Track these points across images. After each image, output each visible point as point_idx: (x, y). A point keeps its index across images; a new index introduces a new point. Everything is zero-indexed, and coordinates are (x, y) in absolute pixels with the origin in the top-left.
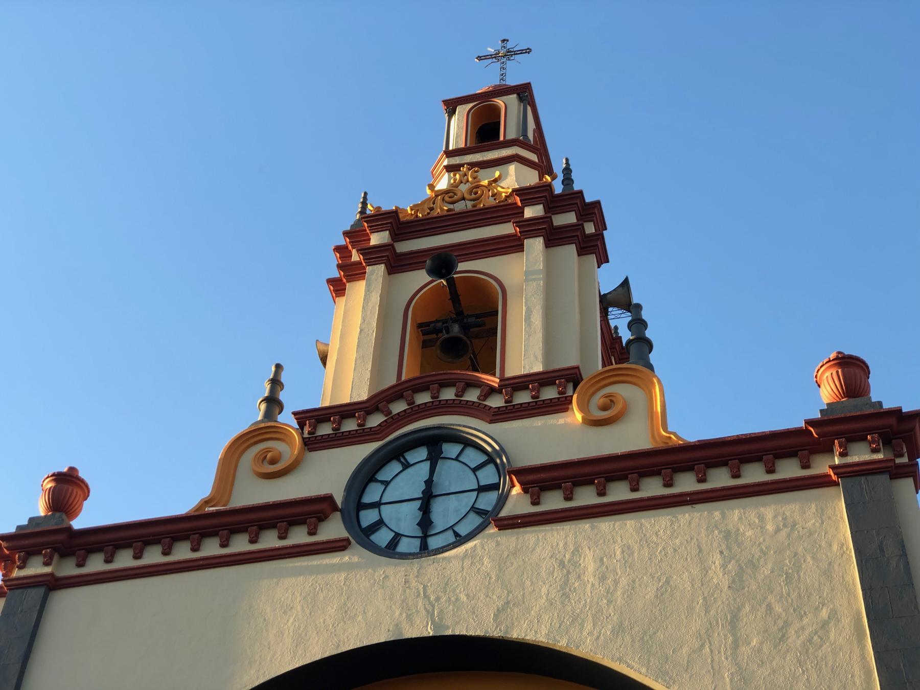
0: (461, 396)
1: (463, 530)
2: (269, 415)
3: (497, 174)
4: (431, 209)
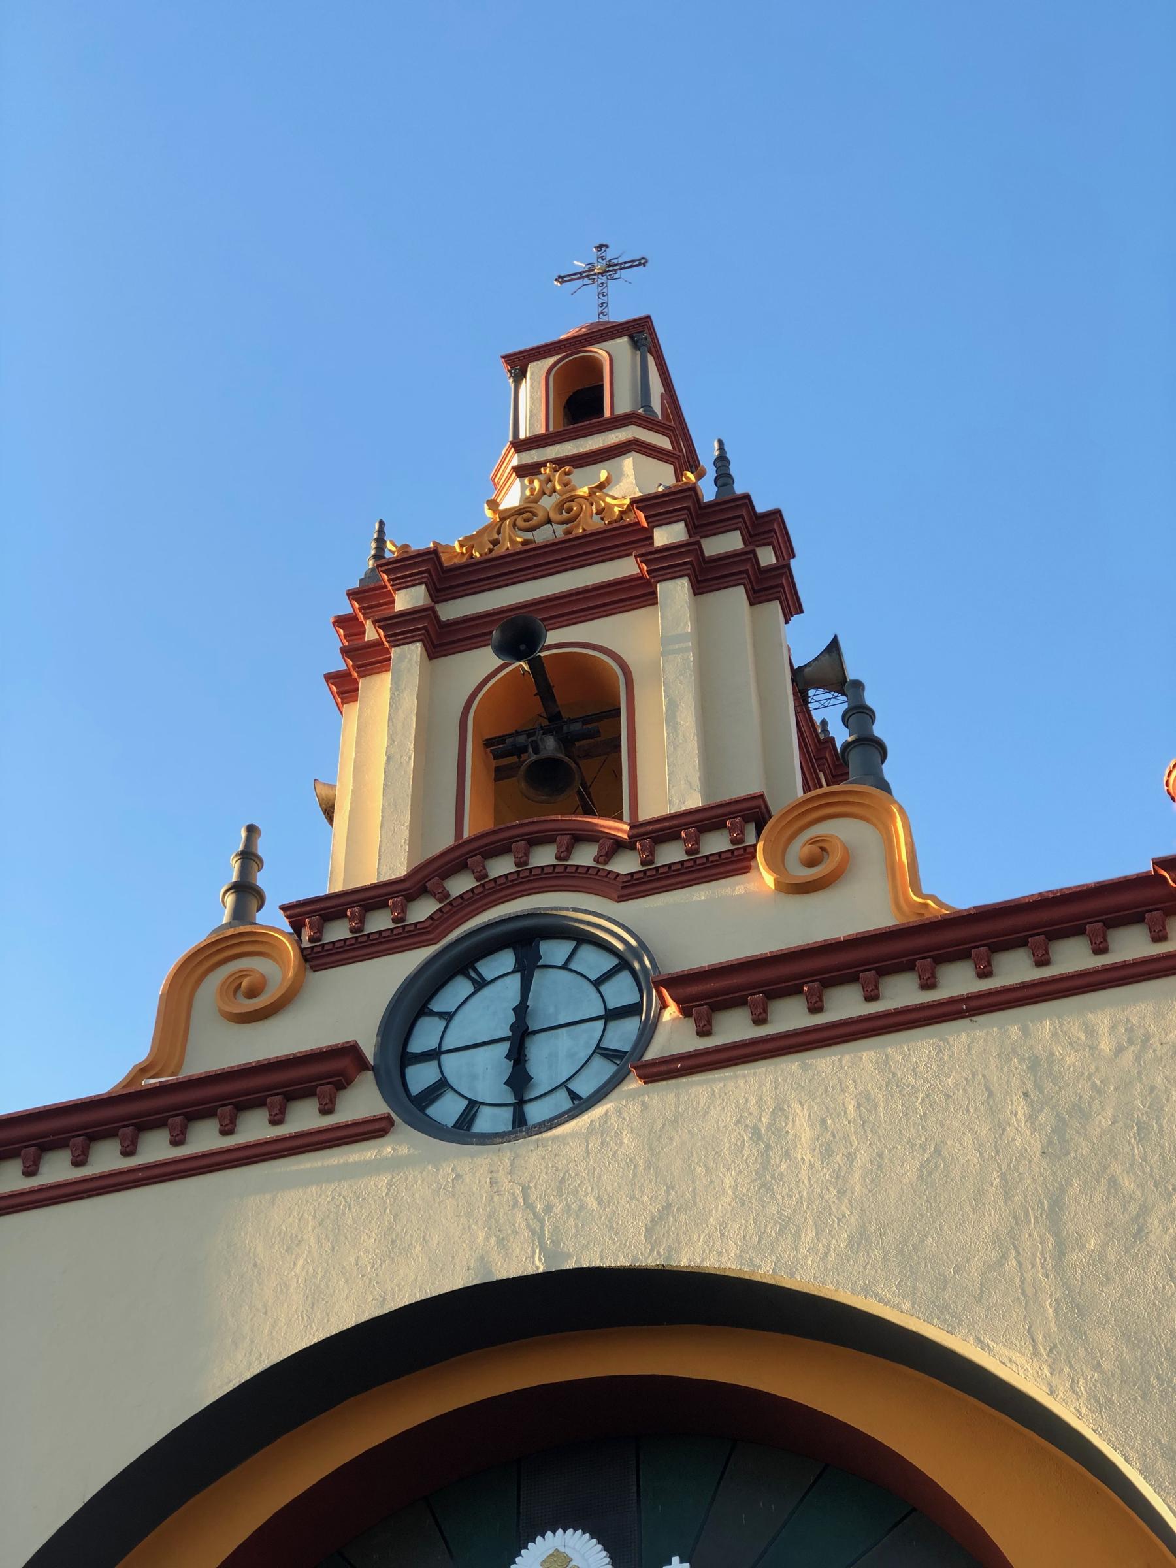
0: (566, 859)
1: (584, 1088)
2: (240, 914)
3: (603, 475)
4: (495, 543)
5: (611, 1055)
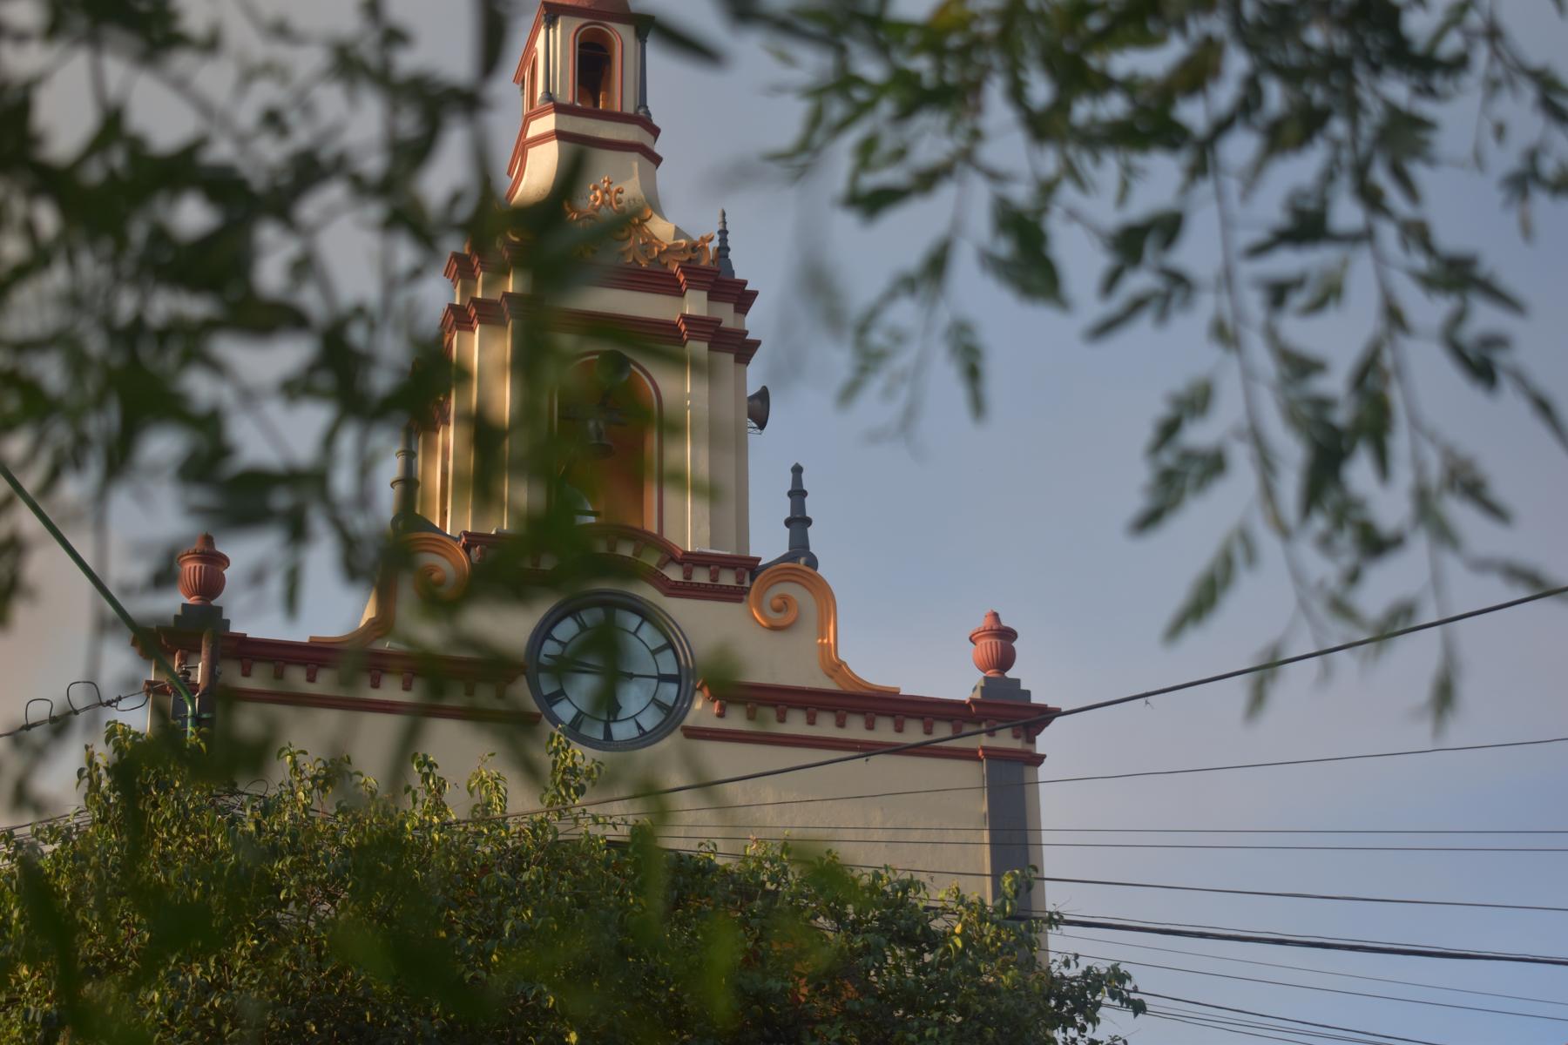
1: (648, 726)
5: (661, 706)
